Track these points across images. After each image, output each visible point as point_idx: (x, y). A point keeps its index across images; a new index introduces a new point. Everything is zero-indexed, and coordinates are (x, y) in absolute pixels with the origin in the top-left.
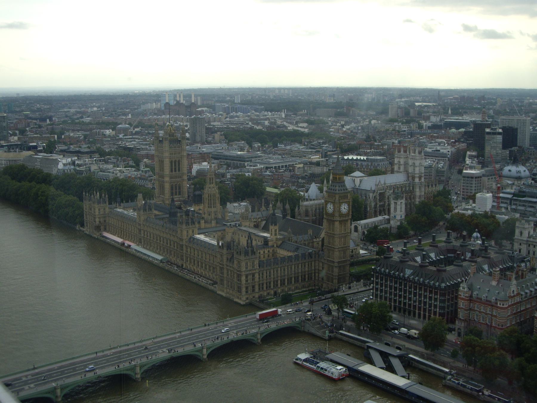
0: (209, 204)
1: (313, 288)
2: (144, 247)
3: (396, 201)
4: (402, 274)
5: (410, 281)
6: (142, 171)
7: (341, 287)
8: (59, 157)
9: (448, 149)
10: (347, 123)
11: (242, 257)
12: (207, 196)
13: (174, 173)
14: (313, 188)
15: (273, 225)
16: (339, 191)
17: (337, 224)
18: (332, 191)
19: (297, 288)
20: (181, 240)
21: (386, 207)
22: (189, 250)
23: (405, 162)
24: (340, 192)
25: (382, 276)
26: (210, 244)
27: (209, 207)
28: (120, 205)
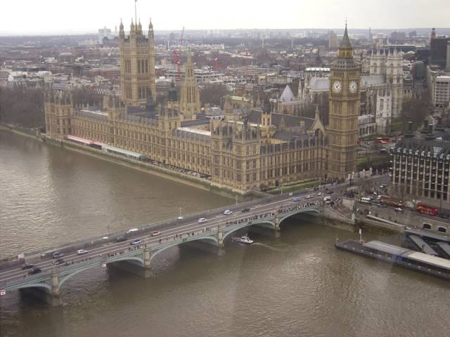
2: (116, 147)
5: (440, 160)
8: (10, 71)
10: (289, 52)
11: (243, 141)
12: (186, 89)
13: (141, 74)
14: (287, 92)
17: (345, 105)
18: (340, 68)
19: (299, 178)
20: (163, 133)
21: (367, 108)
22: (172, 143)
23: (382, 64)
26: (197, 135)
28: (85, 106)
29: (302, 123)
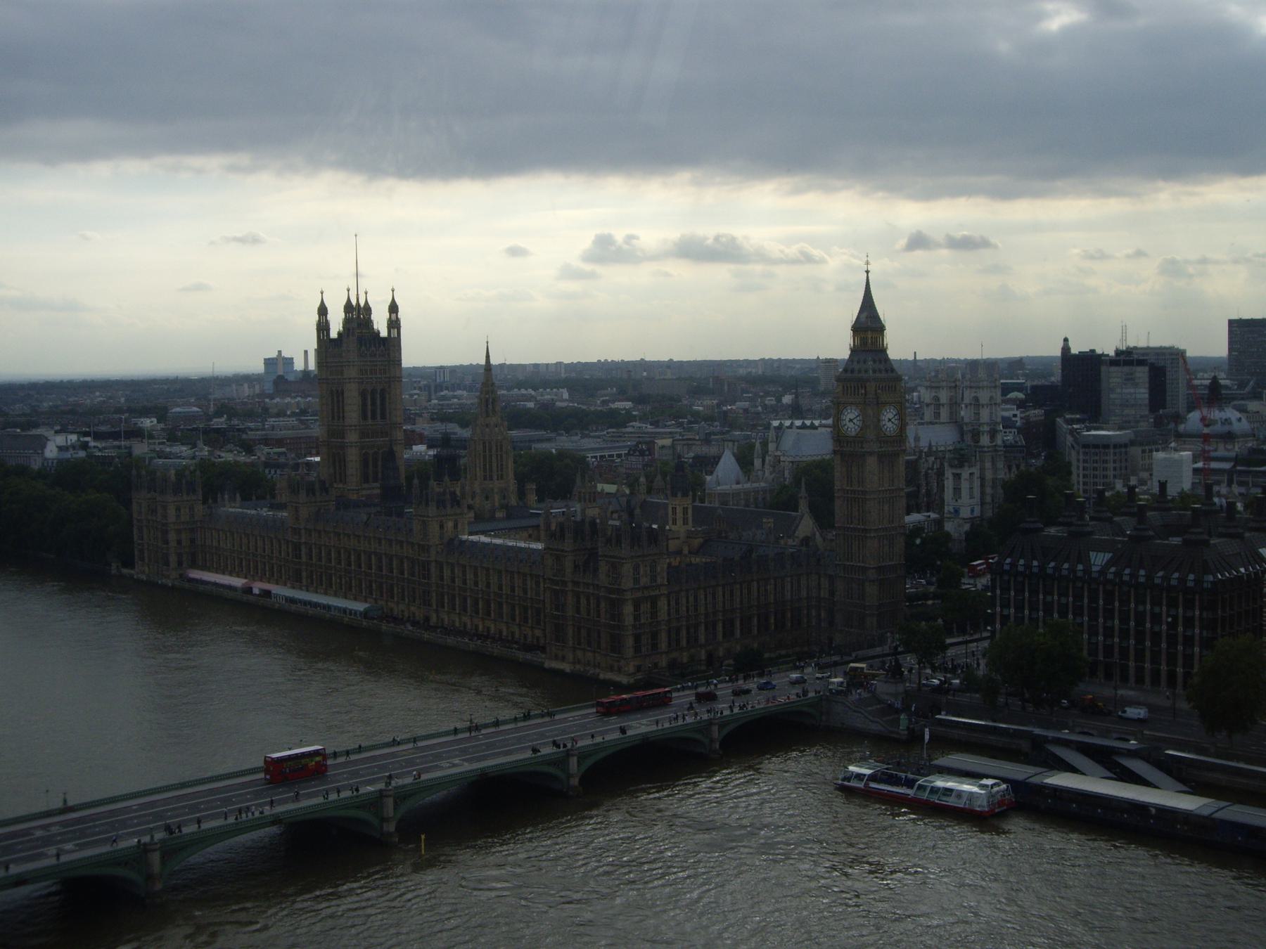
0: (485, 470)
1: (806, 649)
2: (308, 591)
3: (958, 471)
4: (1080, 567)
6: (268, 453)
7: (889, 634)
9: (1013, 409)
13: (370, 422)
15: (679, 495)
16: (874, 371)
17: (872, 462)
23: (951, 400)
24: (878, 375)
25: (1020, 579)
27: (485, 479)
29: (769, 522)
